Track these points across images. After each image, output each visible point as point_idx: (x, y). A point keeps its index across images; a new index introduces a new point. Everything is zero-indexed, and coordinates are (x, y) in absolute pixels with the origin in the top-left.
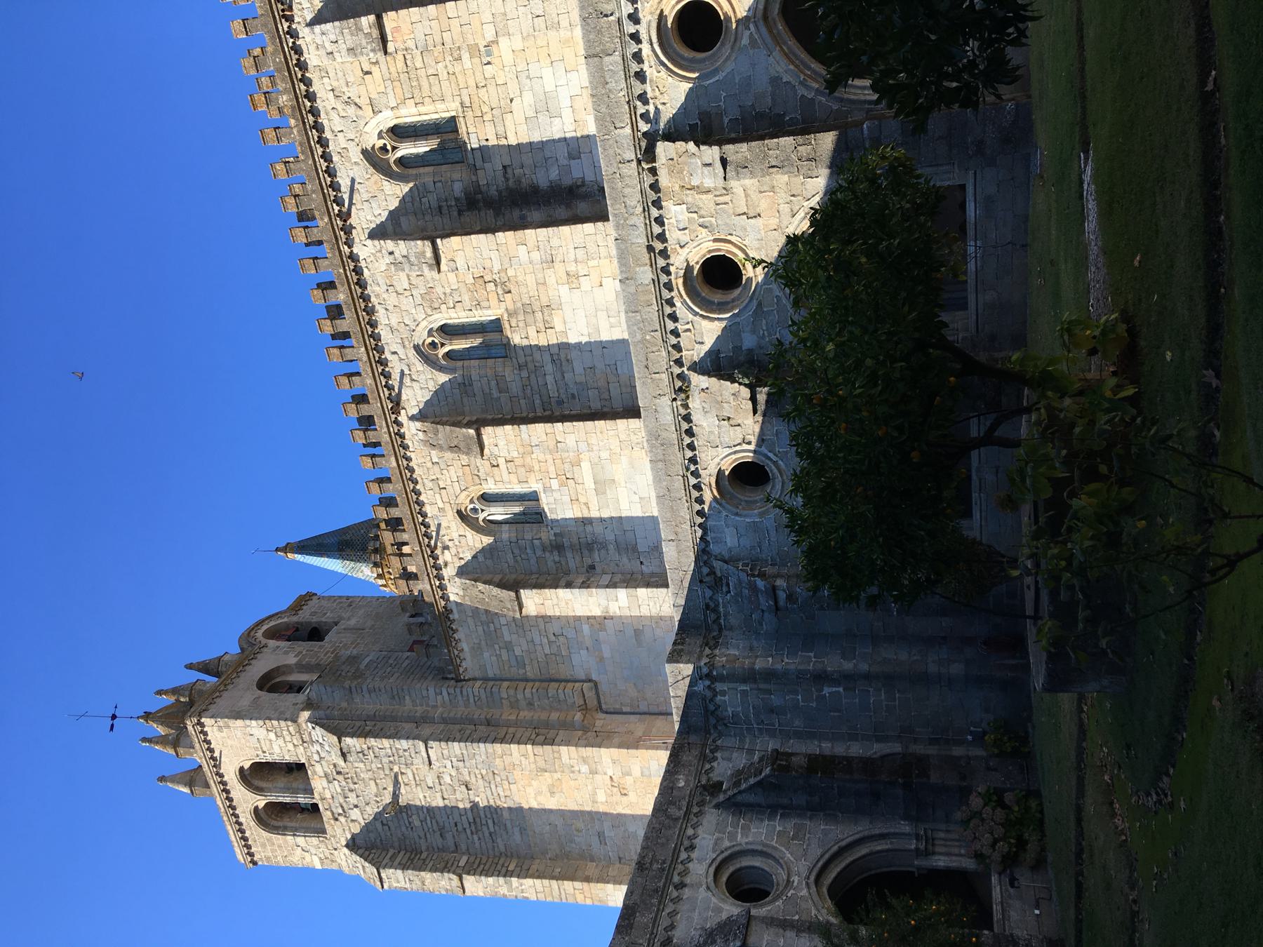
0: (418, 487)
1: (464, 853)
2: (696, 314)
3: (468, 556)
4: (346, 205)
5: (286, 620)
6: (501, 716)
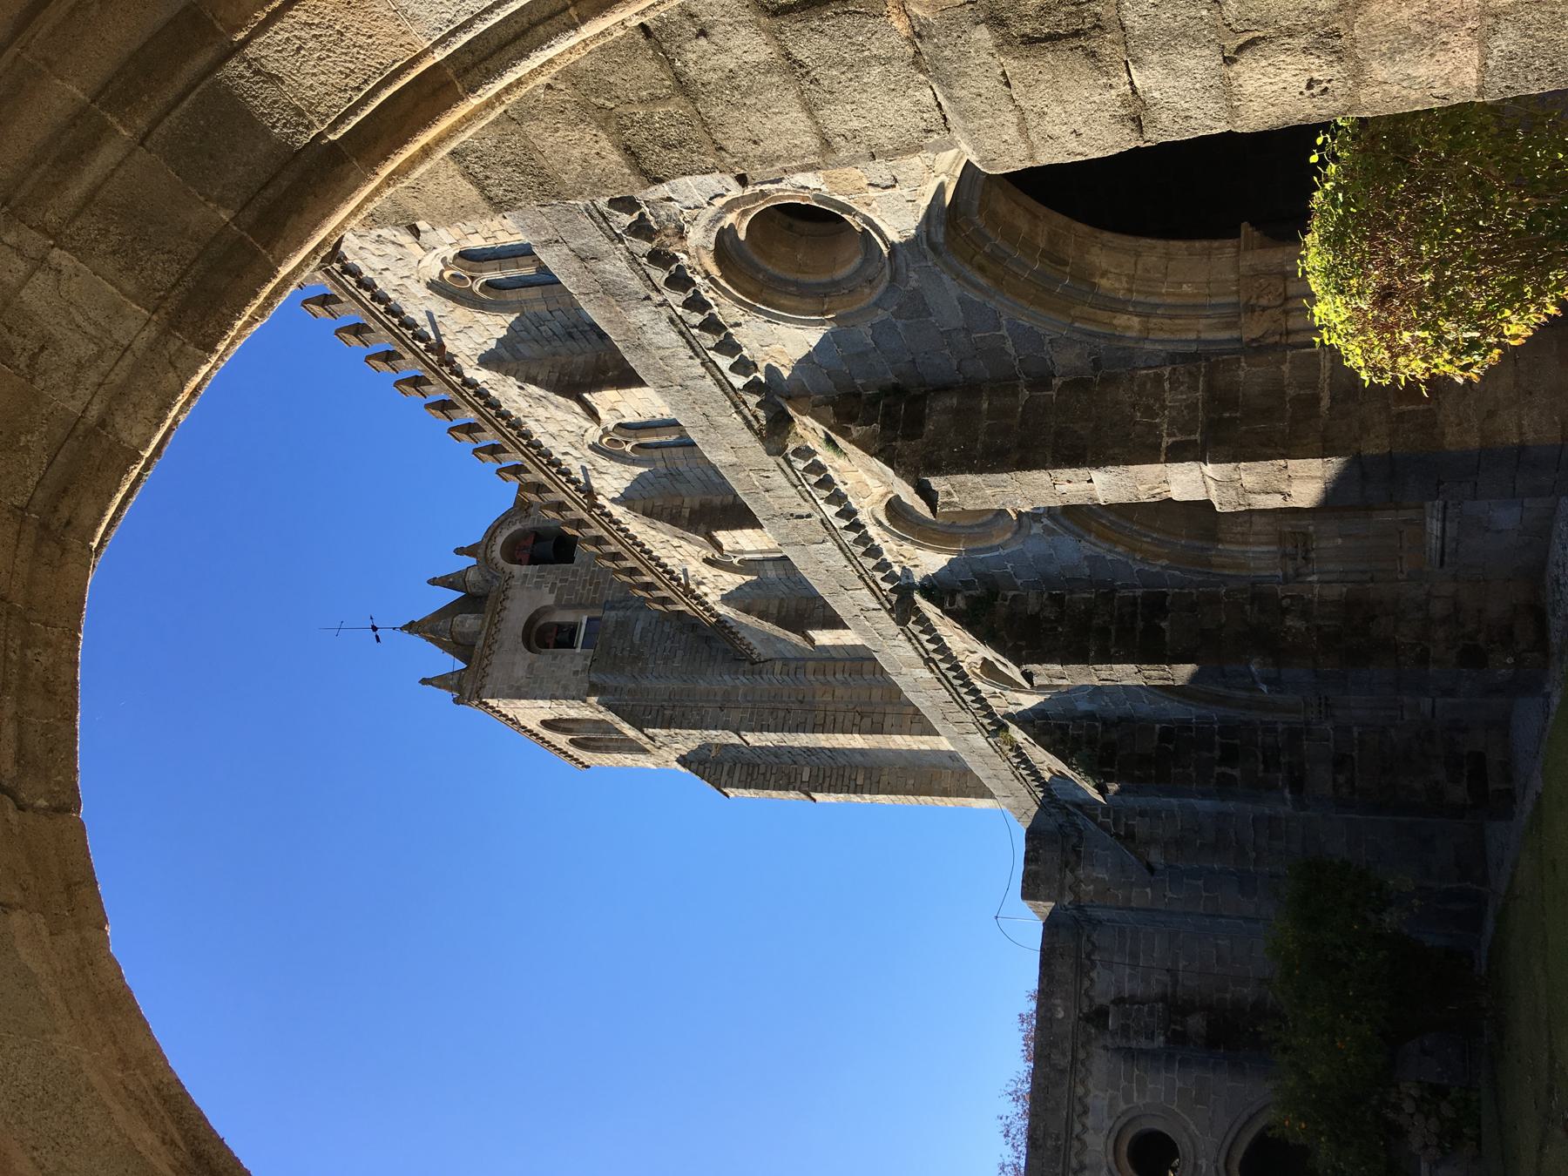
1: (803, 766)
2: (1005, 689)
3: (732, 588)
4: (433, 336)
5: (518, 526)
6: (814, 697)
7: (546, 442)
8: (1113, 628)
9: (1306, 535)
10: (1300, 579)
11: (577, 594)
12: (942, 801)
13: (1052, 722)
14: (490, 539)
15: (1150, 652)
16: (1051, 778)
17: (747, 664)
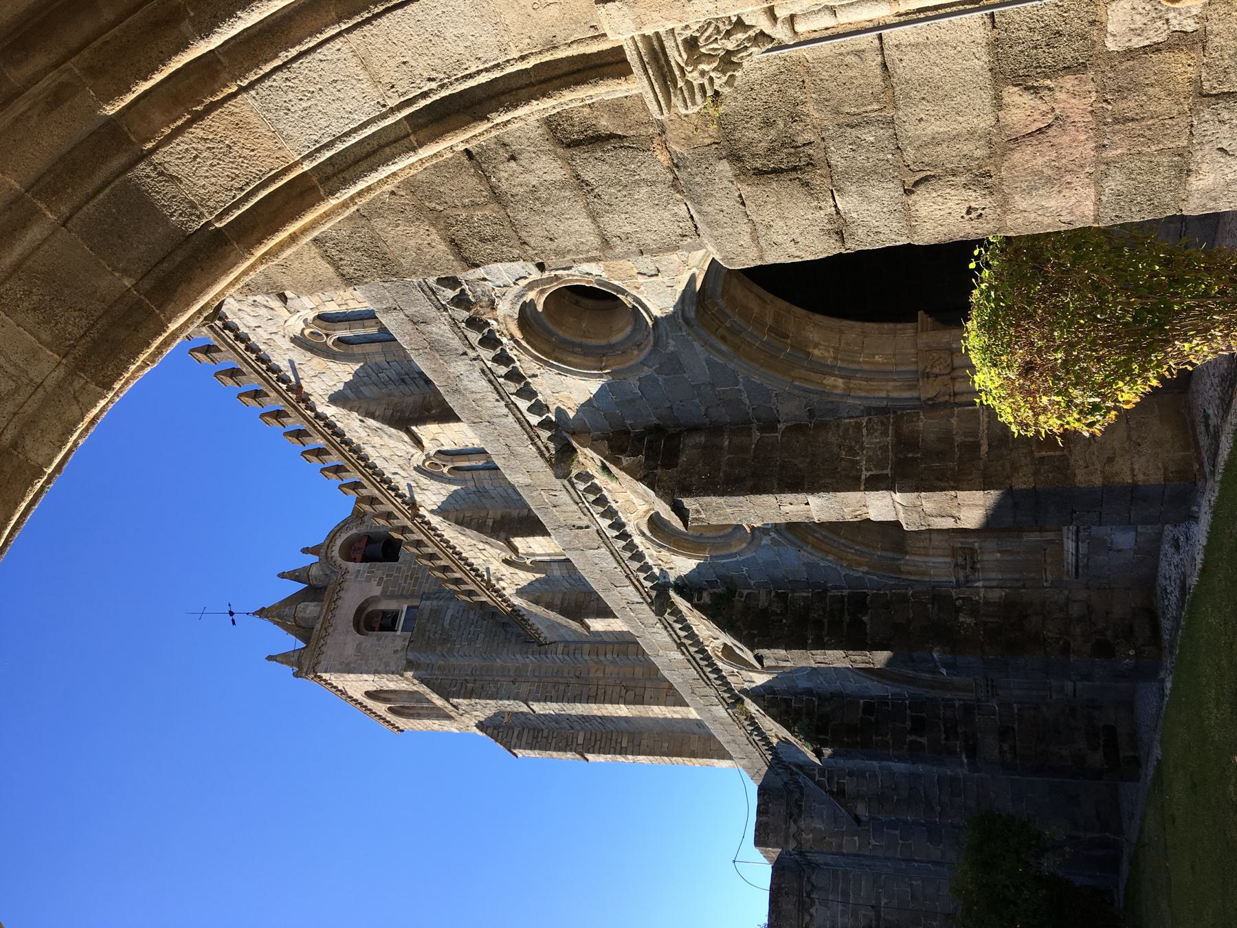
0: (457, 549)
2: (742, 669)
3: (525, 583)
4: (293, 379)
5: (354, 531)
6: (588, 674)
7: (380, 464)
8: (825, 621)
9: (973, 550)
10: (969, 585)
11: (399, 587)
12: (691, 761)
13: (779, 697)
14: (331, 541)
15: (855, 641)
16: (778, 743)
17: (535, 646)
